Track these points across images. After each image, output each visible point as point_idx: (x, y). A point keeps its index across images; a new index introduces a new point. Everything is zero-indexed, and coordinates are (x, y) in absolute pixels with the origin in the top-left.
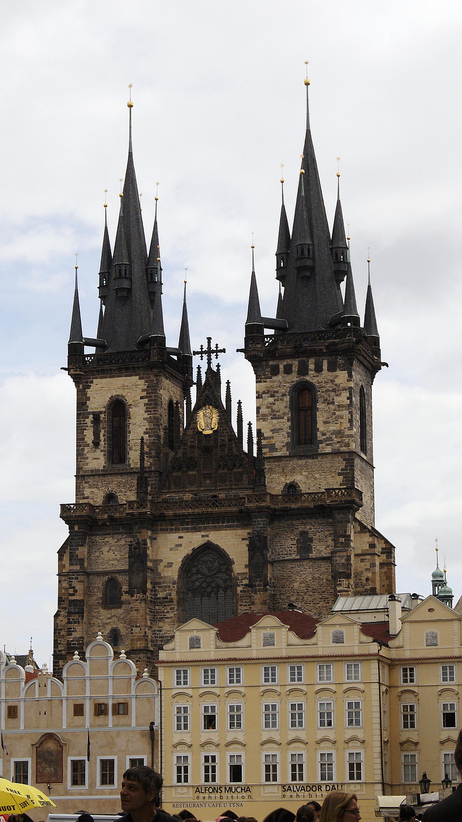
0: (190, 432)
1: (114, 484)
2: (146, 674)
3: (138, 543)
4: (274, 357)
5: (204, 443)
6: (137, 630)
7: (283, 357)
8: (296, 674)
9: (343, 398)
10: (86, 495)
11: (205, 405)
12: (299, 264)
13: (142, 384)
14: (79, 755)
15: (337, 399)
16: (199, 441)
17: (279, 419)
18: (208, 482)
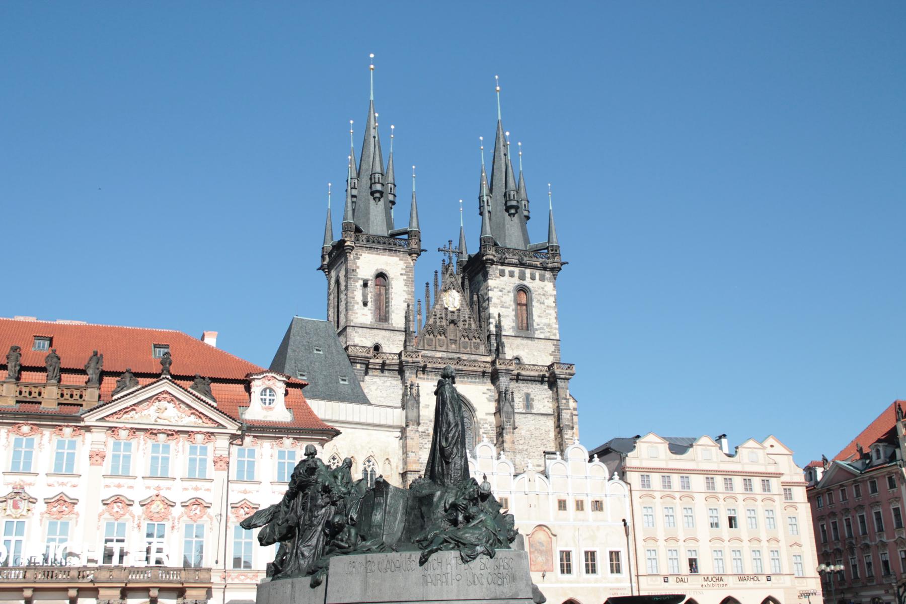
0: (438, 307)
1: (379, 337)
2: (616, 477)
3: (412, 385)
4: (503, 264)
5: (449, 317)
6: (413, 455)
7: (509, 264)
8: (728, 483)
9: (551, 301)
10: (356, 342)
11: (449, 288)
12: (509, 204)
13: (402, 265)
14: (566, 546)
15: (546, 301)
16: (446, 315)
17: (506, 307)
18: (453, 346)
